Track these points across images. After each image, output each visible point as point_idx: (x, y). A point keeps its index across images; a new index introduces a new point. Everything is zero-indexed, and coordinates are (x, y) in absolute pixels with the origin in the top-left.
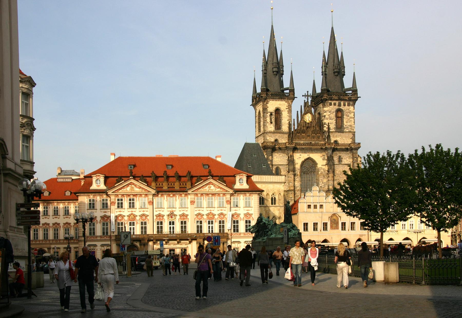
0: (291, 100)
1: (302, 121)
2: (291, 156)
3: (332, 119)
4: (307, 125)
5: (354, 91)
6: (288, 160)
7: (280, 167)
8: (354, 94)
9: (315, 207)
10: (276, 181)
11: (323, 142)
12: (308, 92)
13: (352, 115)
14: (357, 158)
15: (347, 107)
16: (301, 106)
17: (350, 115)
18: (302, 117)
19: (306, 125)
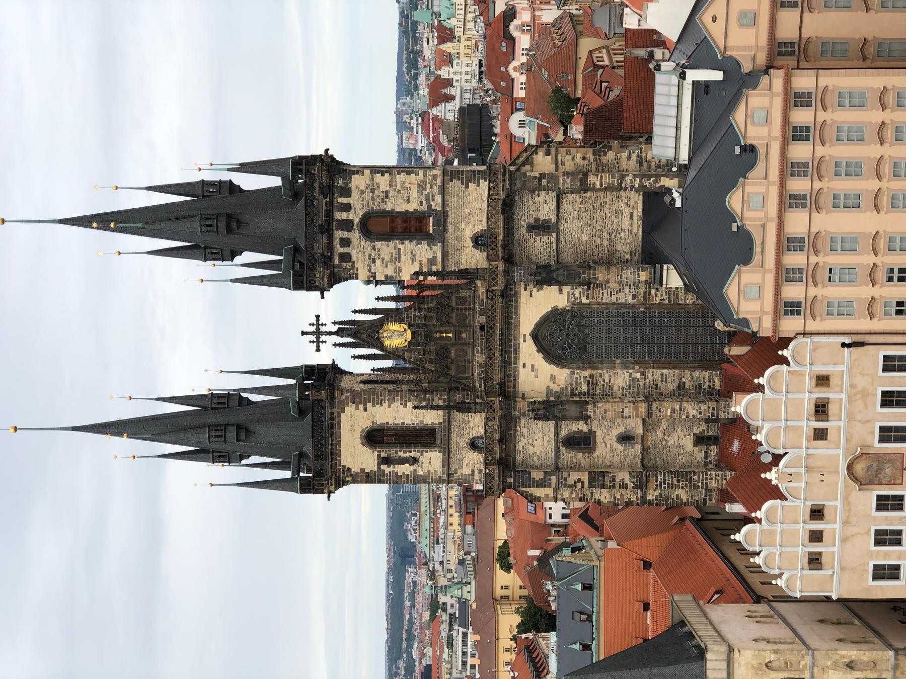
0: (337, 394)
1: (407, 356)
2: (533, 410)
3: (399, 254)
4: (422, 339)
6: (545, 418)
7: (564, 433)
8: (308, 174)
9: (816, 536)
12: (303, 333)
13: (383, 181)
14: (542, 176)
15: (354, 200)
16: (355, 357)
17: (384, 187)
19: (419, 344)
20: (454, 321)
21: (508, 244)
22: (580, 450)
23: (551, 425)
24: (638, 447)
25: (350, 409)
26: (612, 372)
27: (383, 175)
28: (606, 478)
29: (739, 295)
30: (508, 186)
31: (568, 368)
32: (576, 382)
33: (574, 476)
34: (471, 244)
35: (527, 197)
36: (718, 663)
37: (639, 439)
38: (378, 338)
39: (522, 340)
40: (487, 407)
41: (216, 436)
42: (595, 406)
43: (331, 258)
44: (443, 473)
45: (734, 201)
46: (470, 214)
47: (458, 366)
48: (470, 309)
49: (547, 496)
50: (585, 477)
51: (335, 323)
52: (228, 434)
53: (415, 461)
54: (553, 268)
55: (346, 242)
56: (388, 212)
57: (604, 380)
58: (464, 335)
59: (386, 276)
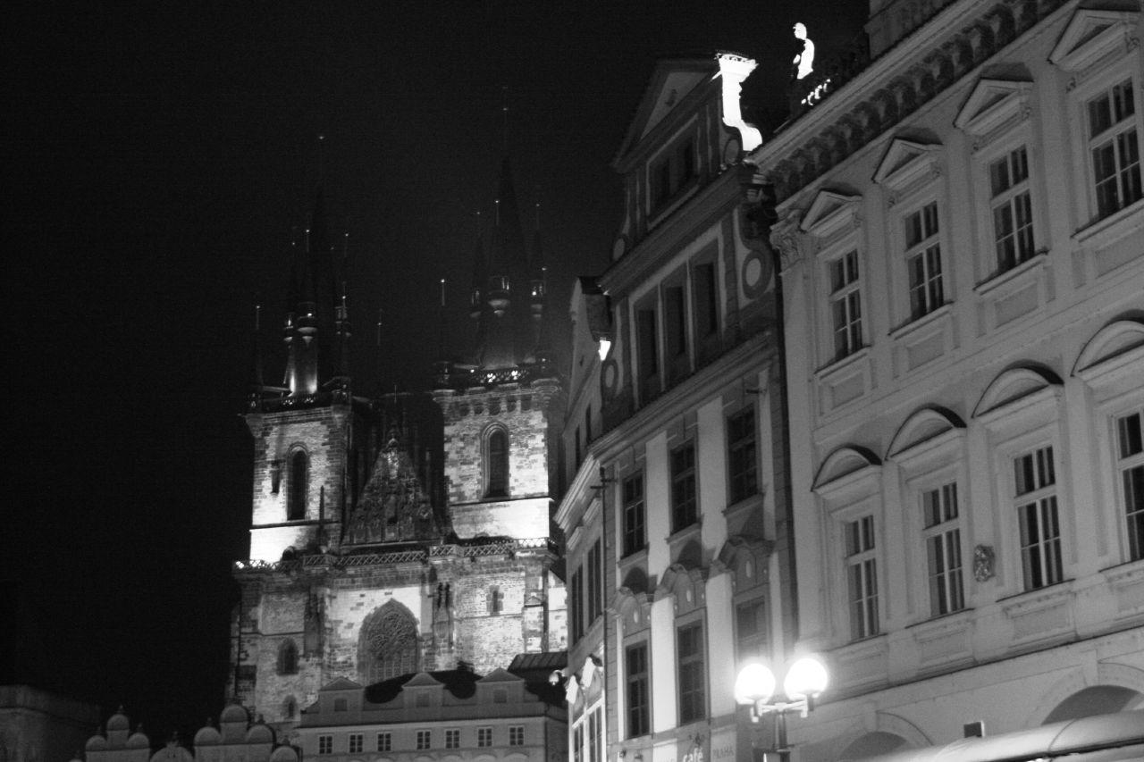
22: (280, 660)
23: (302, 629)
24: (282, 719)
27: (543, 441)
31: (359, 640)
32: (345, 650)
33: (251, 651)
34: (478, 532)
35: (523, 583)
37: (287, 720)
39: (387, 590)
42: (318, 664)
50: (249, 662)
55: (478, 411)
58: (393, 534)
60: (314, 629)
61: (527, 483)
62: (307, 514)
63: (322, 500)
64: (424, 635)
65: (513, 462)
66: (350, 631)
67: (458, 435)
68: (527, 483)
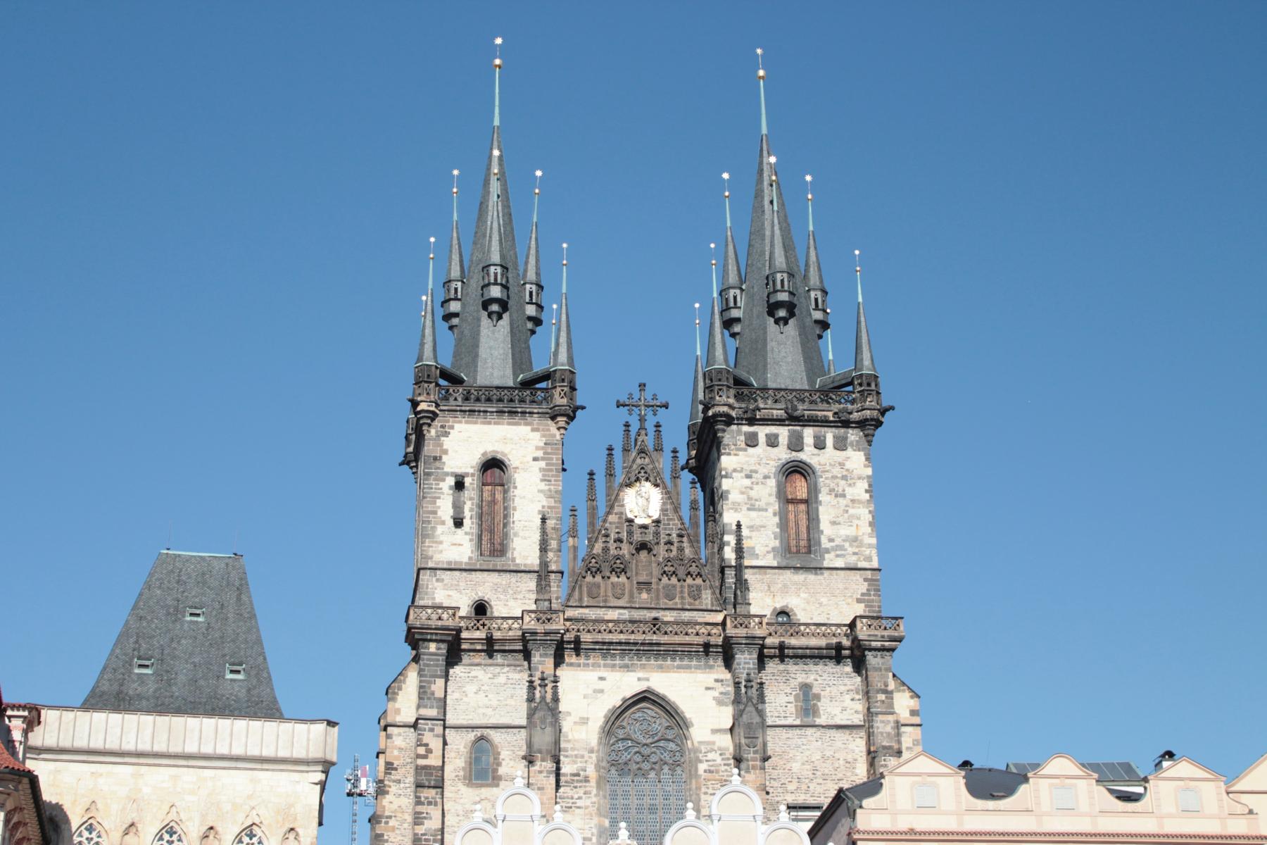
0: (562, 420)
1: (612, 518)
2: (543, 679)
3: (760, 510)
4: (637, 537)
5: (869, 385)
7: (496, 736)
10: (268, 752)
11: (719, 618)
12: (642, 386)
13: (859, 490)
14: (889, 693)
16: (610, 449)
17: (850, 492)
18: (613, 501)
19: (630, 533)
20: (665, 579)
21: (783, 653)
25: (536, 439)
26: (593, 810)
27: (867, 491)
28: (433, 791)
29: (919, 775)
30: (874, 644)
31: (600, 743)
32: (576, 756)
36: (305, 744)
38: (638, 480)
39: (641, 675)
40: (546, 614)
41: (496, 274)
42: (549, 772)
43: (752, 421)
44: (438, 563)
45: (1060, 765)
46: (821, 604)
47: (599, 587)
48: (682, 603)
49: (398, 711)
50: (434, 761)
51: (658, 426)
52: (498, 288)
53: (458, 523)
54: (760, 707)
55: (772, 442)
56: (817, 497)
57: (580, 798)
58: (644, 596)
59: (728, 492)
60: (543, 721)
61: (847, 545)
62: (509, 555)
63: (544, 532)
64: (700, 743)
65: (826, 514)
66: (584, 727)
67: (742, 470)
68: (847, 545)
